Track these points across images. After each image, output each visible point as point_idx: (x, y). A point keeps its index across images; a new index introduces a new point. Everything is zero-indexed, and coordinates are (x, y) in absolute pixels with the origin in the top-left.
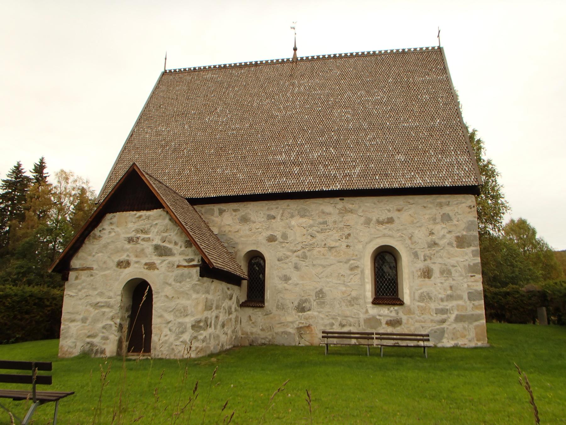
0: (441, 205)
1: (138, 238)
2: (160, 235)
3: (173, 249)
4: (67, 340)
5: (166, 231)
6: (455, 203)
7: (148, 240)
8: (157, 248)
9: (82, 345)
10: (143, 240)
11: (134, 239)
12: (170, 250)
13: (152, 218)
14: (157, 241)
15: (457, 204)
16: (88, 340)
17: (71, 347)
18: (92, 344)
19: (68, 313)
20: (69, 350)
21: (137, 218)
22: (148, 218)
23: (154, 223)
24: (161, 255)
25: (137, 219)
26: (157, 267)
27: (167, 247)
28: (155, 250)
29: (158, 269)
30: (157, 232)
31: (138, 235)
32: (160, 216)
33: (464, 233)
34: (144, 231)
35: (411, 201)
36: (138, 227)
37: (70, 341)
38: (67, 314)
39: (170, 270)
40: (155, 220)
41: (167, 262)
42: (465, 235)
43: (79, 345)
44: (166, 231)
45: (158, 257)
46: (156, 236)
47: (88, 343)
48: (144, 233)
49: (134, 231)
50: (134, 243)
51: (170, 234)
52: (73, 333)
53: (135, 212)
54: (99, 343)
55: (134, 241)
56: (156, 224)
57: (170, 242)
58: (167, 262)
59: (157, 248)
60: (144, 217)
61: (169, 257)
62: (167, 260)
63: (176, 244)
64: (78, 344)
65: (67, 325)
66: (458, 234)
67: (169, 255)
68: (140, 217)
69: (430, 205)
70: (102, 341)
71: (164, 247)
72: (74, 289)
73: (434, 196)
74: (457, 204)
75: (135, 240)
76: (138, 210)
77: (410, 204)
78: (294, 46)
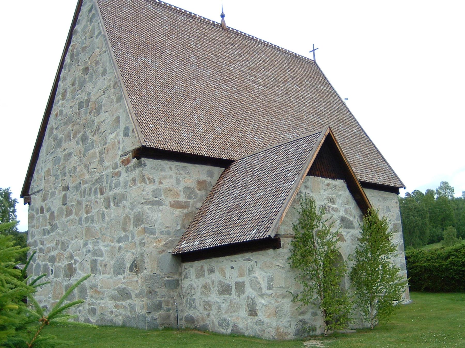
0: (385, 199)
1: (329, 207)
2: (343, 207)
3: (353, 222)
4: (281, 320)
5: (347, 203)
6: (390, 198)
7: (336, 210)
8: (343, 220)
9: (296, 323)
10: (333, 209)
11: (327, 207)
12: (351, 223)
13: (338, 188)
14: (342, 213)
15: (391, 200)
16: (301, 317)
17: (286, 327)
18: (303, 322)
19: (281, 287)
20: (284, 331)
21: (326, 185)
22: (335, 187)
23: (340, 193)
24: (346, 227)
25: (326, 187)
26: (345, 239)
27: (350, 220)
28: (341, 221)
29: (346, 241)
30: (342, 203)
31: (329, 204)
32: (343, 186)
33: (396, 222)
34: (332, 201)
35: (372, 194)
36: (328, 196)
37: (285, 321)
38: (278, 289)
39: (353, 242)
40: (340, 190)
41: (350, 234)
42: (397, 223)
43: (293, 323)
44: (347, 203)
45: (344, 229)
46: (340, 207)
47: (301, 321)
48: (332, 203)
49: (325, 199)
50: (327, 212)
51: (350, 207)
52: (287, 311)
53: (323, 179)
54: (310, 319)
55: (327, 211)
56: (341, 194)
57: (351, 215)
58: (350, 234)
59: (343, 220)
60: (331, 186)
61: (352, 229)
62: (350, 232)
63: (355, 217)
64: (292, 323)
65: (280, 301)
66: (394, 222)
67: (351, 228)
68: (328, 185)
69: (381, 199)
70: (312, 317)
71: (348, 219)
72: (281, 259)
73: (382, 192)
74: (391, 200)
75: (327, 209)
76: (326, 177)
77: (372, 196)
78: (221, 13)
